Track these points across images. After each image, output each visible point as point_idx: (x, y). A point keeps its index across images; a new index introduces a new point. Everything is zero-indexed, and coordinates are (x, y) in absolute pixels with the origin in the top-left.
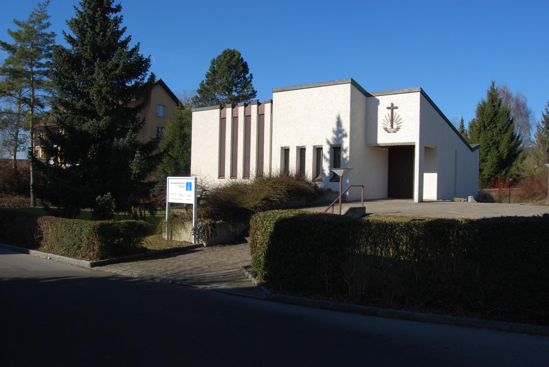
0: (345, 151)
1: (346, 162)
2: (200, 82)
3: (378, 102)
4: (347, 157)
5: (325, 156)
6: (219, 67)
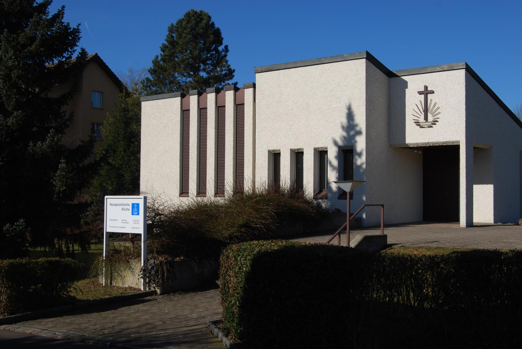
0: (360, 155)
1: (361, 171)
2: (153, 58)
3: (405, 84)
4: (362, 164)
5: (330, 163)
6: (180, 36)
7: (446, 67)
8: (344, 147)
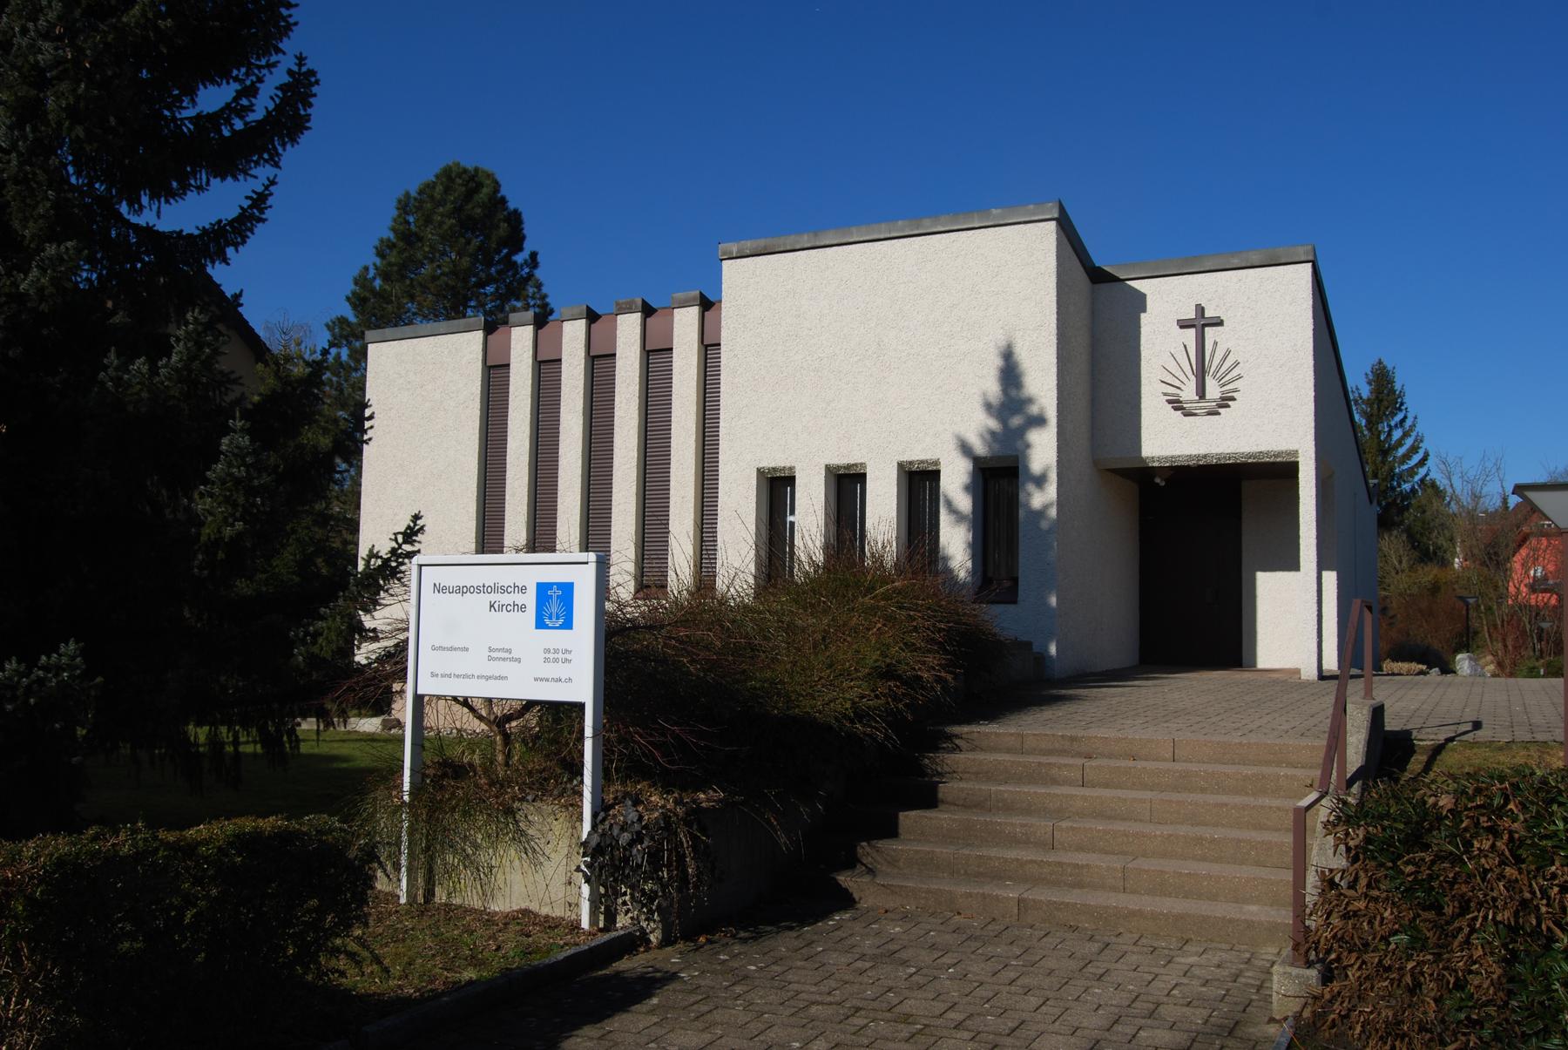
0: (1040, 481)
1: (1044, 525)
2: (356, 272)
3: (1139, 302)
4: (1046, 507)
5: (949, 504)
6: (428, 221)
7: (1255, 259)
8: (992, 458)
